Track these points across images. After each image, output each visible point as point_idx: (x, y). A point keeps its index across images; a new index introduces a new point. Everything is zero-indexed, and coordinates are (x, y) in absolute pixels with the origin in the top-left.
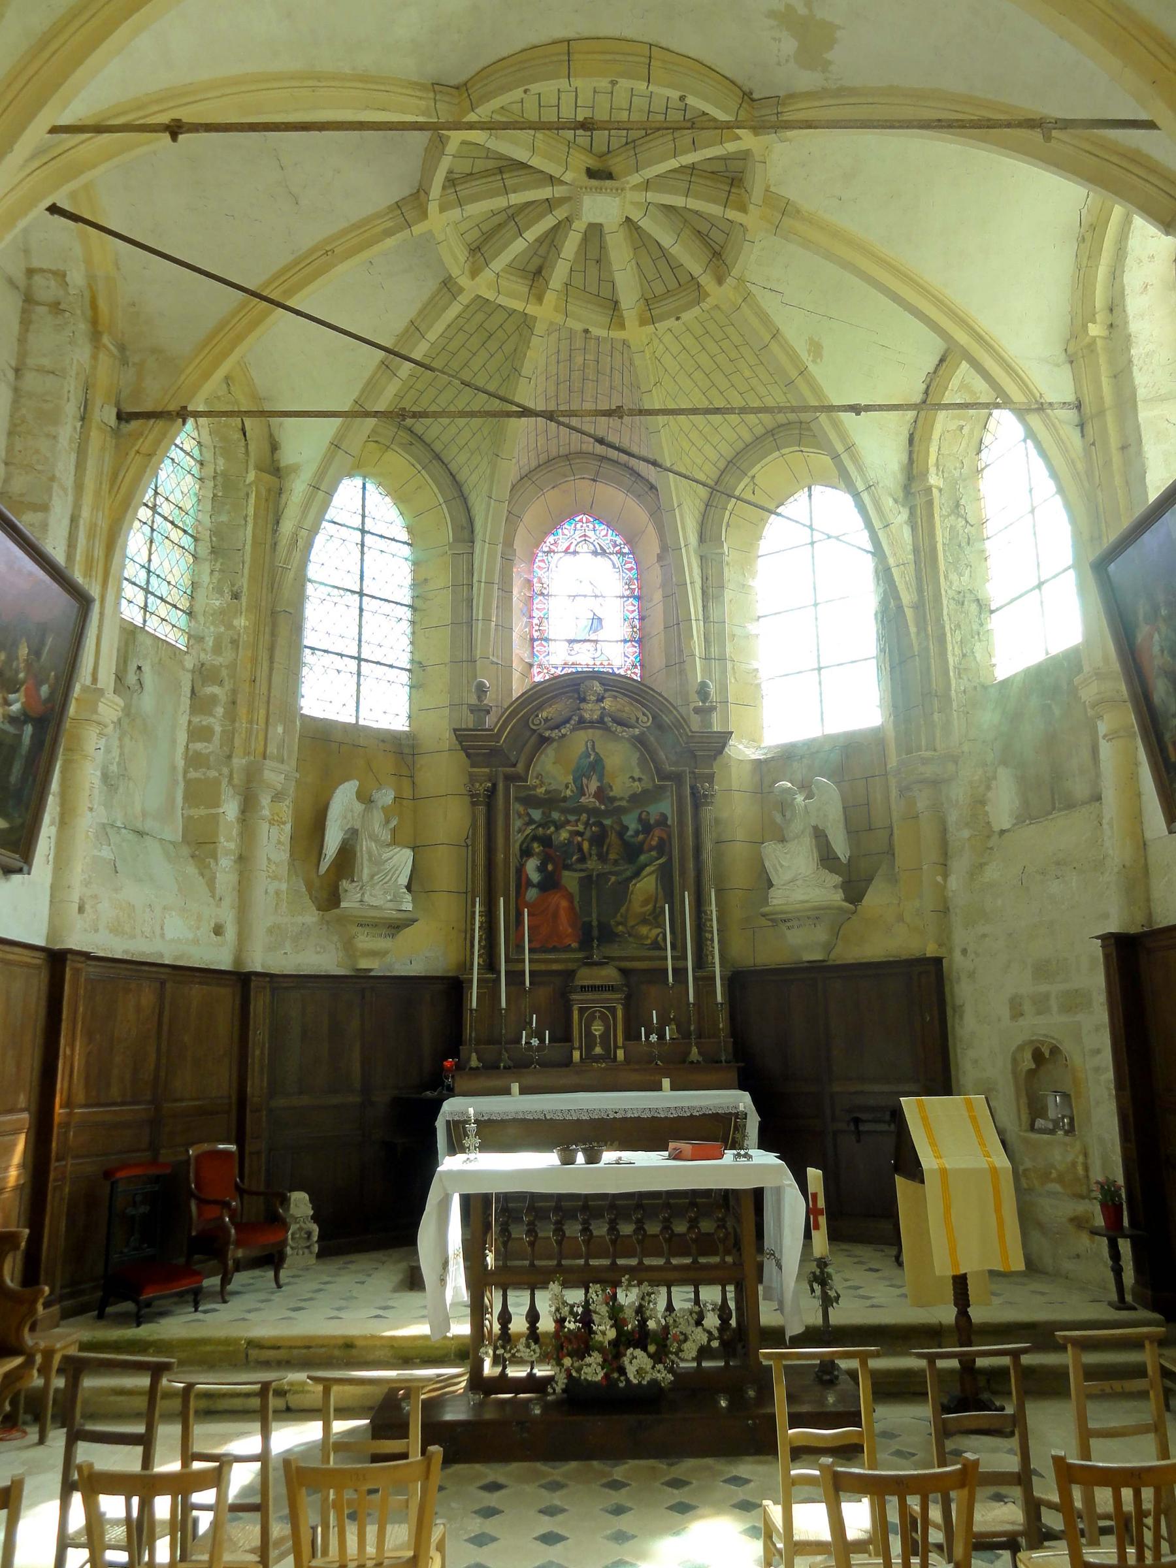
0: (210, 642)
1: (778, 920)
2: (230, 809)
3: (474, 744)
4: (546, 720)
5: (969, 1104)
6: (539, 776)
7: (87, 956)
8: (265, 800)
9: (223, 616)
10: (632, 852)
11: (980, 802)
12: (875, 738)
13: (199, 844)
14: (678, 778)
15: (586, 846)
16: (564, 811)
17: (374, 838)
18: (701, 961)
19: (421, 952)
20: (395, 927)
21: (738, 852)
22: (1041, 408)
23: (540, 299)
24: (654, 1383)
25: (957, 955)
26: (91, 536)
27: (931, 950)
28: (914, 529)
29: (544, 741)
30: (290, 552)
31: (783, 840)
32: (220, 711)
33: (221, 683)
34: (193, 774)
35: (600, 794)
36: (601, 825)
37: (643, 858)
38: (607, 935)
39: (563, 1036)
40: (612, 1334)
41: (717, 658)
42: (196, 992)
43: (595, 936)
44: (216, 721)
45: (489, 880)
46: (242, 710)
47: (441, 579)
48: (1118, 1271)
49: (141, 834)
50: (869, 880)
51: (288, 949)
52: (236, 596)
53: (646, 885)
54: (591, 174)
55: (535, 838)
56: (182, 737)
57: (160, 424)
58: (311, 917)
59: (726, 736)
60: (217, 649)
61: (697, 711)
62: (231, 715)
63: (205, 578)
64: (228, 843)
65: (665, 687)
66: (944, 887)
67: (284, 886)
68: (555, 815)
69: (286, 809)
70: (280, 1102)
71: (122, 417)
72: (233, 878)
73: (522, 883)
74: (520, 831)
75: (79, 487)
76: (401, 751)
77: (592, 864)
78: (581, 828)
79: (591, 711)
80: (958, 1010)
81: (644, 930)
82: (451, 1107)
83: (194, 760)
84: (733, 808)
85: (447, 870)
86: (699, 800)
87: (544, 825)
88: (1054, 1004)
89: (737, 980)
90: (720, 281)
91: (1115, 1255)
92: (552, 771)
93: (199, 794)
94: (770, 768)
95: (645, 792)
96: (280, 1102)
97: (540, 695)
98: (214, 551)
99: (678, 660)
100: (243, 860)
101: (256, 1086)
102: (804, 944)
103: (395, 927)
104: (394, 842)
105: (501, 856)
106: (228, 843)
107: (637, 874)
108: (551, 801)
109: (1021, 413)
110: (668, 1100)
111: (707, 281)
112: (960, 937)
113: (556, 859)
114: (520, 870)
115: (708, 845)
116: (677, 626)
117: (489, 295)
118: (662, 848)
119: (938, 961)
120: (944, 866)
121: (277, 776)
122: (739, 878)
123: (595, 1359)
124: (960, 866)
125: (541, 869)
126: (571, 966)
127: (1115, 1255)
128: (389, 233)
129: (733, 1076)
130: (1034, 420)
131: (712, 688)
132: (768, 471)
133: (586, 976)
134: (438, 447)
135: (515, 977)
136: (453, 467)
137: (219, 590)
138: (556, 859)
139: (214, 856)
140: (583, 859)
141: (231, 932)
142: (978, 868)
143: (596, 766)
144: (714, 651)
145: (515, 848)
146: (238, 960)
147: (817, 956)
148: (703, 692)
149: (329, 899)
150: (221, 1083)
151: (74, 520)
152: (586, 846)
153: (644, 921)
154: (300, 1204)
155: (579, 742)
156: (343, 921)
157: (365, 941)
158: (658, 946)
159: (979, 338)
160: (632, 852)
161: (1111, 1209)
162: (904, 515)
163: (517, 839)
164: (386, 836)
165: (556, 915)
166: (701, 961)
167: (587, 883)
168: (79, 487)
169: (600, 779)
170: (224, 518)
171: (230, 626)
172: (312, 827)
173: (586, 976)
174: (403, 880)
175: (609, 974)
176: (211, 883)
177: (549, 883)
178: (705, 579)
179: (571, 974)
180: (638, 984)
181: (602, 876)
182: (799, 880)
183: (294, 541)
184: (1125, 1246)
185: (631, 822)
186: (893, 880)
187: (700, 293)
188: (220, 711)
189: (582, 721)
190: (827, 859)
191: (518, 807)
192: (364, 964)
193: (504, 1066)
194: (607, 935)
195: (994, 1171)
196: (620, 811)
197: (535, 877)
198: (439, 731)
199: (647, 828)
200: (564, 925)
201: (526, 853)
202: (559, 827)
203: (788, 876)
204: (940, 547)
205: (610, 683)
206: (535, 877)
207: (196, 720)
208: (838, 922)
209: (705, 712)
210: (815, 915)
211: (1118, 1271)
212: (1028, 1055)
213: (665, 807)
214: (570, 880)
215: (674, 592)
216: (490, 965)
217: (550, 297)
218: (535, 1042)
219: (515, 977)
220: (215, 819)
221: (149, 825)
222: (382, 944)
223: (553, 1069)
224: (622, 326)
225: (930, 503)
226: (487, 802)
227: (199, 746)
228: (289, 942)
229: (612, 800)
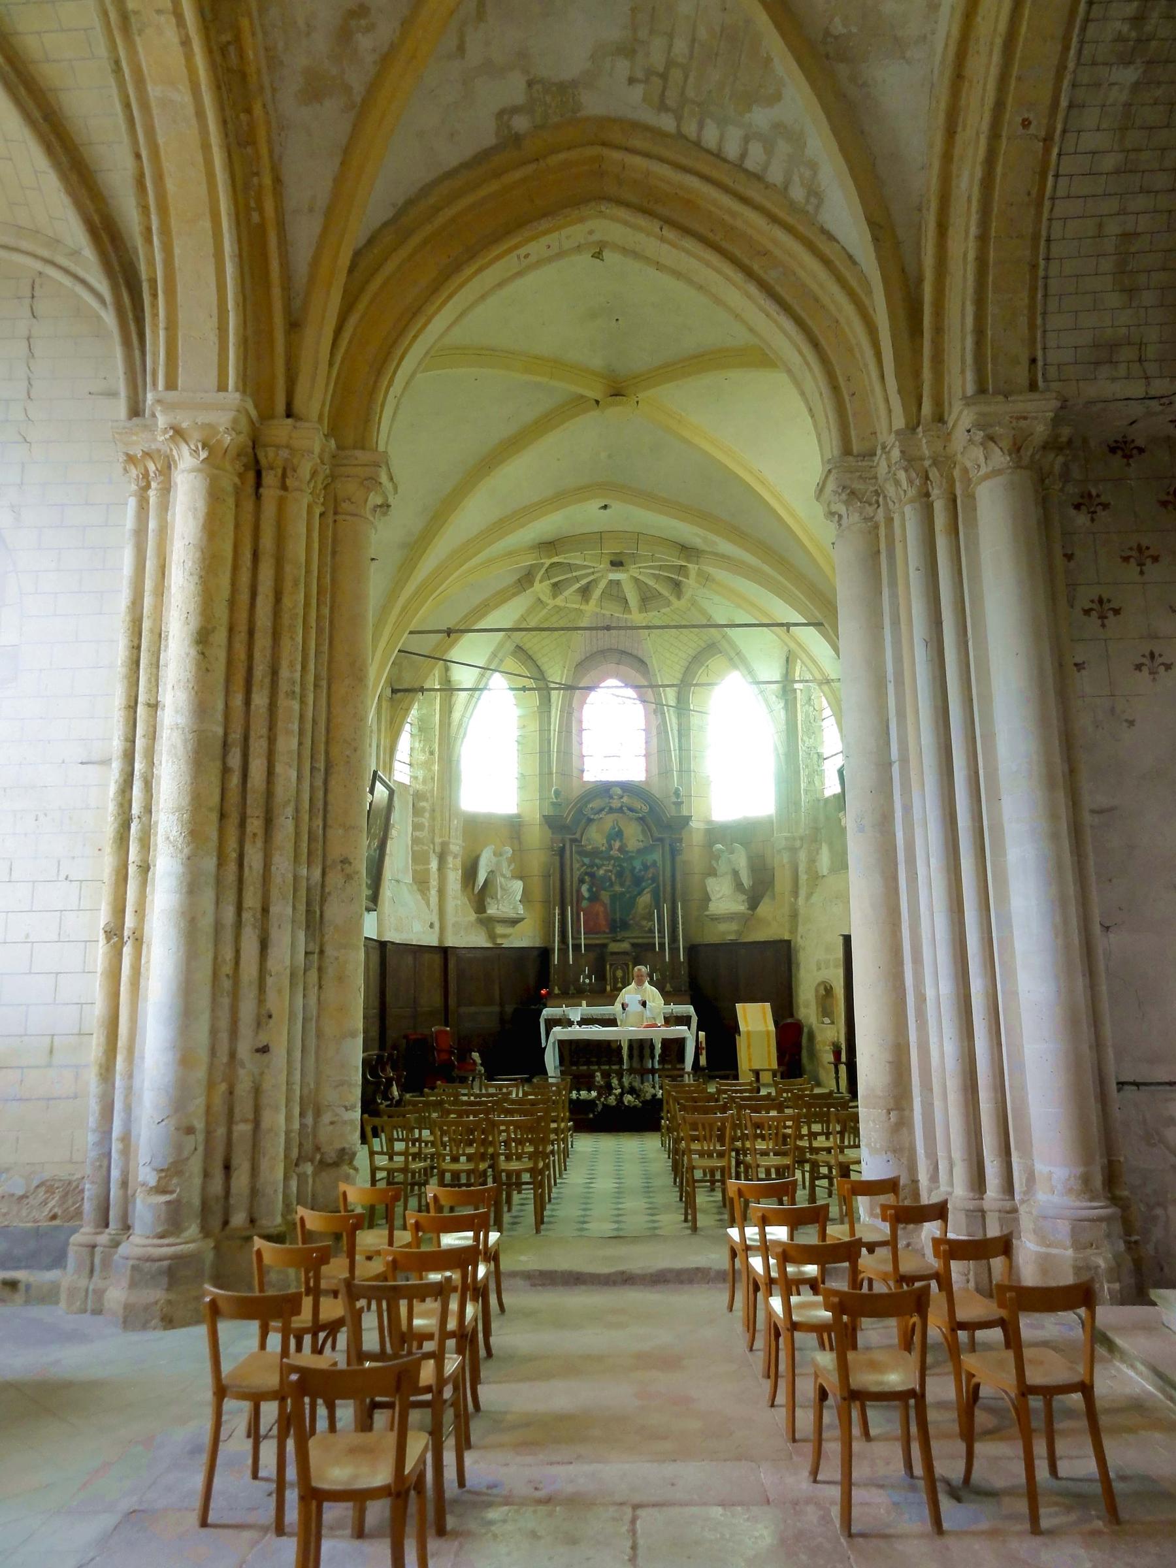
0: (421, 778)
1: (715, 919)
2: (434, 865)
3: (552, 822)
4: (592, 809)
5: (764, 1009)
6: (588, 839)
7: (393, 943)
8: (450, 859)
9: (427, 765)
11: (812, 861)
12: (769, 822)
13: (421, 882)
14: (661, 840)
15: (613, 878)
16: (601, 859)
17: (504, 876)
22: (828, 682)
23: (587, 601)
24: (635, 1107)
25: (799, 938)
26: (384, 753)
27: (786, 938)
28: (787, 710)
29: (590, 821)
30: (458, 729)
31: (715, 875)
32: (427, 815)
33: (427, 801)
34: (416, 848)
35: (620, 850)
36: (620, 866)
37: (644, 884)
38: (625, 925)
39: (601, 977)
40: (619, 1091)
41: (685, 771)
42: (427, 957)
44: (425, 820)
46: (438, 814)
47: (534, 726)
48: (837, 1079)
49: (398, 881)
50: (762, 897)
51: (462, 933)
52: (432, 753)
53: (645, 899)
54: (613, 564)
55: (587, 874)
56: (410, 829)
57: (411, 694)
58: (473, 916)
59: (689, 818)
60: (424, 782)
61: (674, 803)
62: (433, 818)
63: (417, 745)
64: (434, 883)
65: (656, 790)
66: (795, 903)
67: (459, 902)
68: (597, 861)
69: (458, 862)
70: (463, 1010)
71: (394, 691)
72: (437, 900)
74: (578, 869)
75: (379, 730)
77: (618, 888)
78: (610, 868)
79: (616, 804)
80: (798, 965)
81: (644, 923)
82: (547, 1012)
83: (415, 841)
84: (693, 854)
86: (674, 853)
87: (592, 866)
88: (831, 964)
89: (693, 950)
90: (679, 598)
91: (837, 1072)
92: (595, 837)
93: (419, 858)
95: (646, 848)
96: (463, 1010)
98: (420, 730)
99: (665, 772)
100: (441, 892)
101: (452, 1001)
102: (726, 932)
103: (514, 922)
104: (515, 877)
105: (568, 884)
106: (434, 883)
107: (640, 893)
108: (595, 853)
109: (820, 684)
111: (673, 599)
112: (801, 929)
114: (579, 891)
115: (678, 877)
116: (663, 751)
117: (562, 604)
118: (654, 879)
119: (789, 942)
120: (796, 893)
121: (456, 847)
123: (612, 1097)
124: (803, 892)
125: (589, 890)
126: (605, 941)
127: (837, 1072)
128: (514, 595)
129: (688, 998)
130: (825, 688)
131: (682, 792)
132: (715, 663)
134: (530, 653)
135: (577, 947)
136: (539, 663)
137: (423, 750)
139: (428, 889)
140: (612, 885)
141: (437, 925)
142: (809, 896)
143: (619, 834)
144: (685, 767)
145: (575, 880)
146: (441, 939)
147: (732, 937)
148: (677, 793)
149: (480, 907)
150: (437, 999)
151: (378, 746)
152: (613, 878)
153: (644, 918)
154: (476, 1056)
155: (609, 821)
157: (500, 930)
158: (652, 931)
159: (800, 645)
160: (638, 881)
161: (837, 1054)
162: (782, 705)
163: (577, 874)
164: (509, 875)
165: (597, 914)
167: (614, 898)
168: (379, 730)
169: (621, 840)
170: (424, 711)
171: (430, 770)
173: (614, 947)
174: (519, 897)
175: (625, 946)
176: (428, 905)
177: (594, 898)
178: (680, 725)
179: (605, 946)
181: (623, 894)
182: (724, 898)
183: (460, 724)
184: (843, 1068)
186: (773, 898)
187: (669, 604)
188: (427, 815)
189: (611, 808)
190: (739, 886)
191: (575, 856)
192: (499, 941)
193: (573, 994)
194: (625, 925)
195: (768, 1032)
196: (632, 858)
197: (586, 894)
198: (533, 814)
199: (646, 867)
200: (603, 922)
201: (582, 881)
202: (599, 868)
203: (718, 896)
204: (799, 722)
205: (627, 788)
206: (586, 894)
207: (416, 820)
209: (679, 804)
210: (731, 917)
211: (837, 1079)
212: (822, 988)
213: (656, 856)
214: (605, 896)
215: (662, 731)
217: (592, 602)
218: (587, 981)
219: (577, 947)
220: (428, 871)
221: (400, 877)
222: (509, 930)
224: (630, 612)
225: (795, 698)
227: (418, 833)
228: (466, 935)
229: (627, 852)
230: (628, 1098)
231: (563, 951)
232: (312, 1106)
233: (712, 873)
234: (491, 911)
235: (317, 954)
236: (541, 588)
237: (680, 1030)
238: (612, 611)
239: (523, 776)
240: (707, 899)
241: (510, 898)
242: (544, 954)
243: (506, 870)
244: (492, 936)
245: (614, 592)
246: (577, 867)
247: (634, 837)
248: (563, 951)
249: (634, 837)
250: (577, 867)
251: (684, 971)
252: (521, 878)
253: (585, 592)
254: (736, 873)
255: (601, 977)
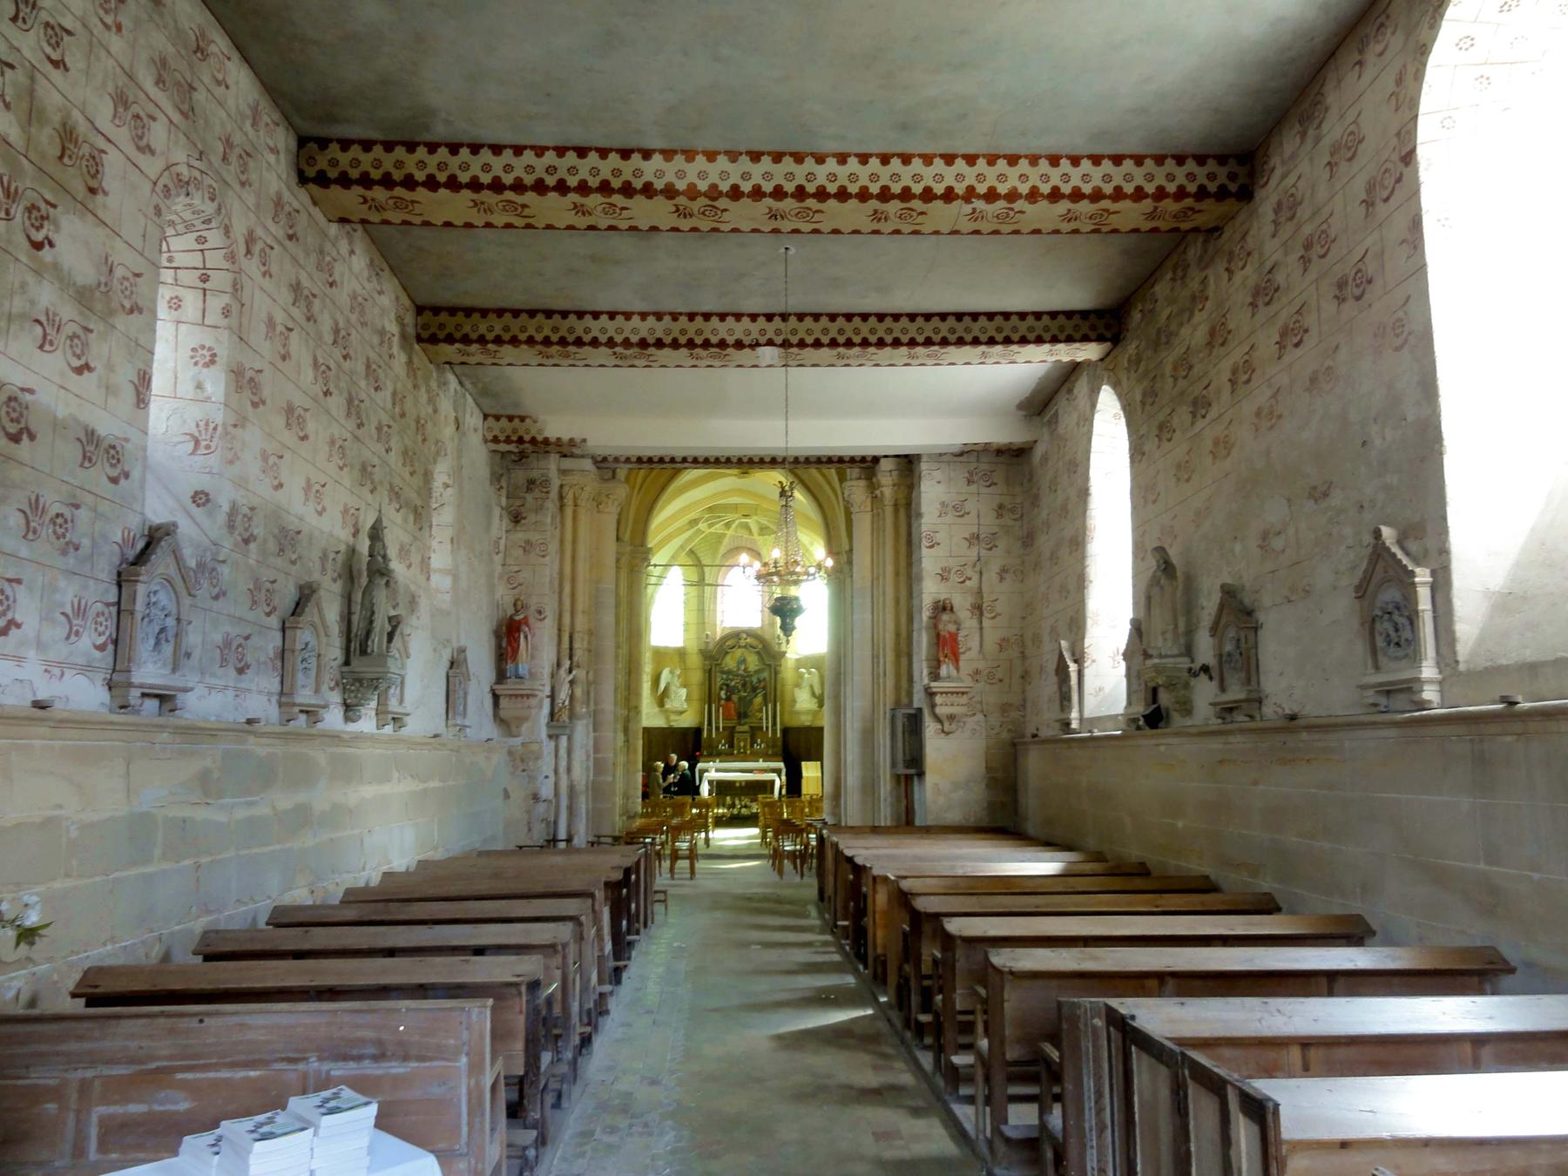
1: (798, 713)
3: (705, 654)
10: (754, 689)
18: (774, 724)
19: (687, 721)
20: (681, 713)
21: (788, 688)
39: (731, 746)
43: (742, 716)
45: (709, 698)
53: (759, 699)
65: (767, 637)
73: (720, 699)
76: (681, 653)
79: (742, 643)
82: (700, 766)
85: (696, 695)
86: (776, 673)
89: (786, 731)
92: (730, 662)
94: (800, 663)
97: (725, 638)
102: (806, 721)
103: (681, 713)
108: (729, 672)
110: (761, 764)
113: (730, 690)
118: (764, 688)
122: (788, 698)
133: (740, 728)
135: (717, 728)
138: (730, 690)
143: (744, 661)
156: (667, 711)
157: (673, 717)
160: (754, 689)
166: (774, 724)
172: (656, 681)
175: (746, 728)
177: (728, 699)
180: (755, 731)
185: (755, 680)
190: (813, 694)
193: (714, 754)
194: (745, 715)
198: (693, 647)
199: (759, 681)
205: (750, 633)
208: (815, 714)
210: (808, 712)
213: (765, 675)
214: (735, 698)
216: (710, 724)
219: (717, 728)
223: (728, 755)
226: (709, 674)
230: (744, 811)
231: (710, 731)
232: (626, 796)
233: (798, 685)
234: (668, 706)
235: (627, 741)
236: (701, 526)
237: (774, 776)
238: (743, 533)
239: (686, 624)
240: (794, 701)
241: (679, 697)
242: (698, 731)
243: (677, 682)
244: (667, 718)
245: (747, 527)
246: (719, 680)
247: (753, 662)
248: (710, 731)
249: (753, 662)
250: (719, 680)
251: (780, 743)
252: (685, 686)
253: (728, 525)
254: (811, 687)
255: (731, 746)
